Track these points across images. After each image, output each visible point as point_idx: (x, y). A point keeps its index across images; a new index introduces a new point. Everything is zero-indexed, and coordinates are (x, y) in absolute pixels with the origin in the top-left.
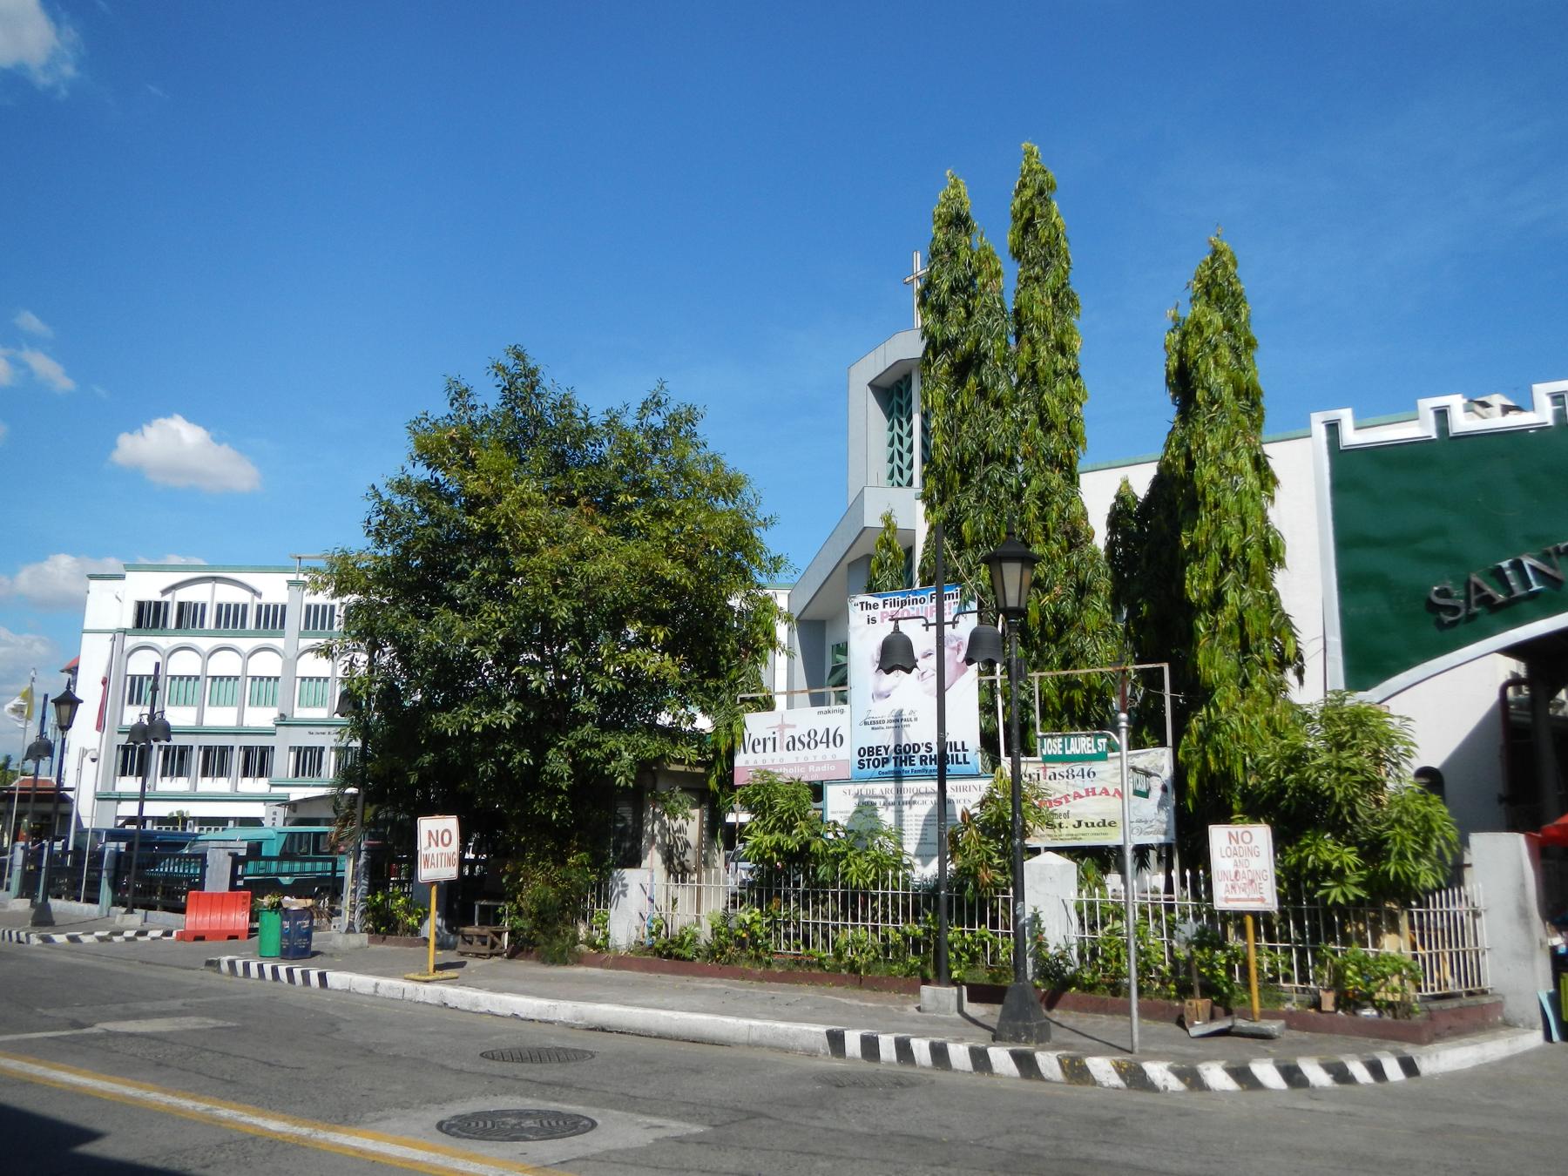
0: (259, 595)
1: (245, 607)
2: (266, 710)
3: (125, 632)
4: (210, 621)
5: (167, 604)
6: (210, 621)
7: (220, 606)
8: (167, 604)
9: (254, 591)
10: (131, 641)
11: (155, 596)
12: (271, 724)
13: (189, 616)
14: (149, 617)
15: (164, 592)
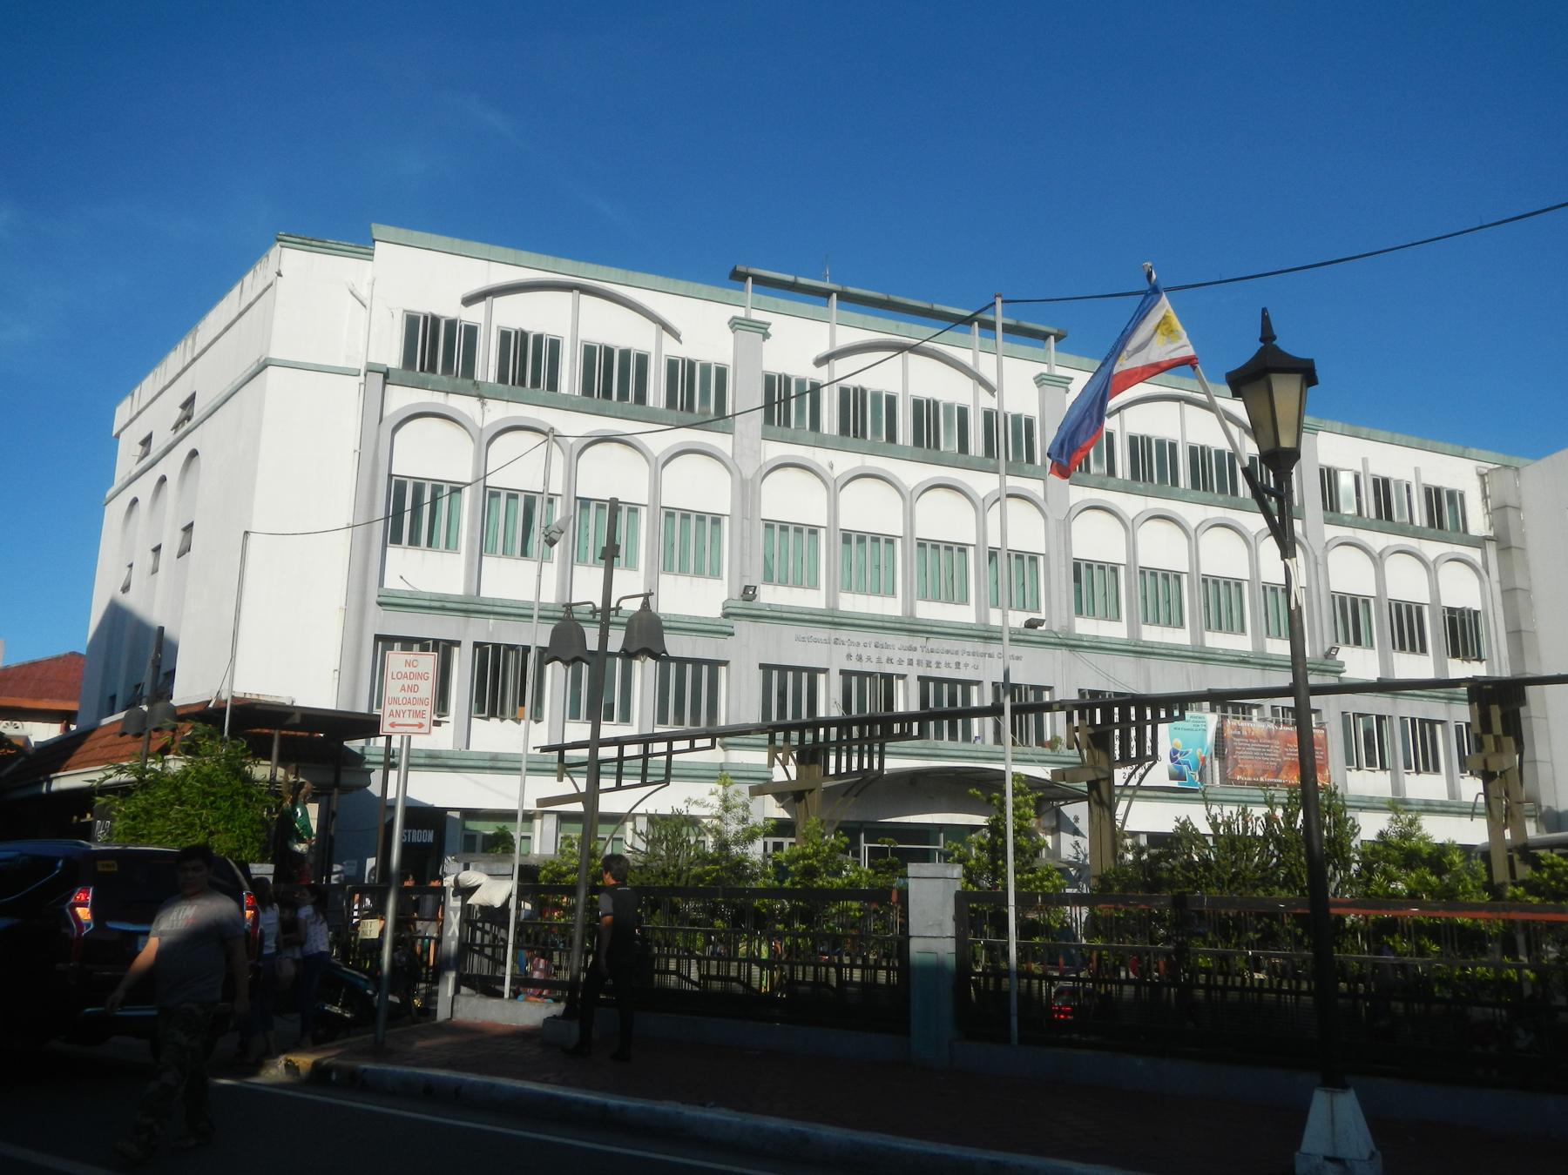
0: (676, 335)
1: (643, 360)
2: (713, 583)
3: (386, 375)
4: (569, 379)
5: (471, 332)
6: (569, 379)
7: (589, 351)
8: (471, 332)
9: (666, 327)
10: (402, 398)
11: (448, 307)
12: (716, 612)
13: (528, 363)
14: (435, 349)
15: (468, 301)
